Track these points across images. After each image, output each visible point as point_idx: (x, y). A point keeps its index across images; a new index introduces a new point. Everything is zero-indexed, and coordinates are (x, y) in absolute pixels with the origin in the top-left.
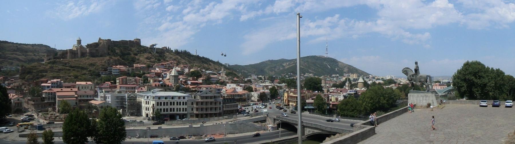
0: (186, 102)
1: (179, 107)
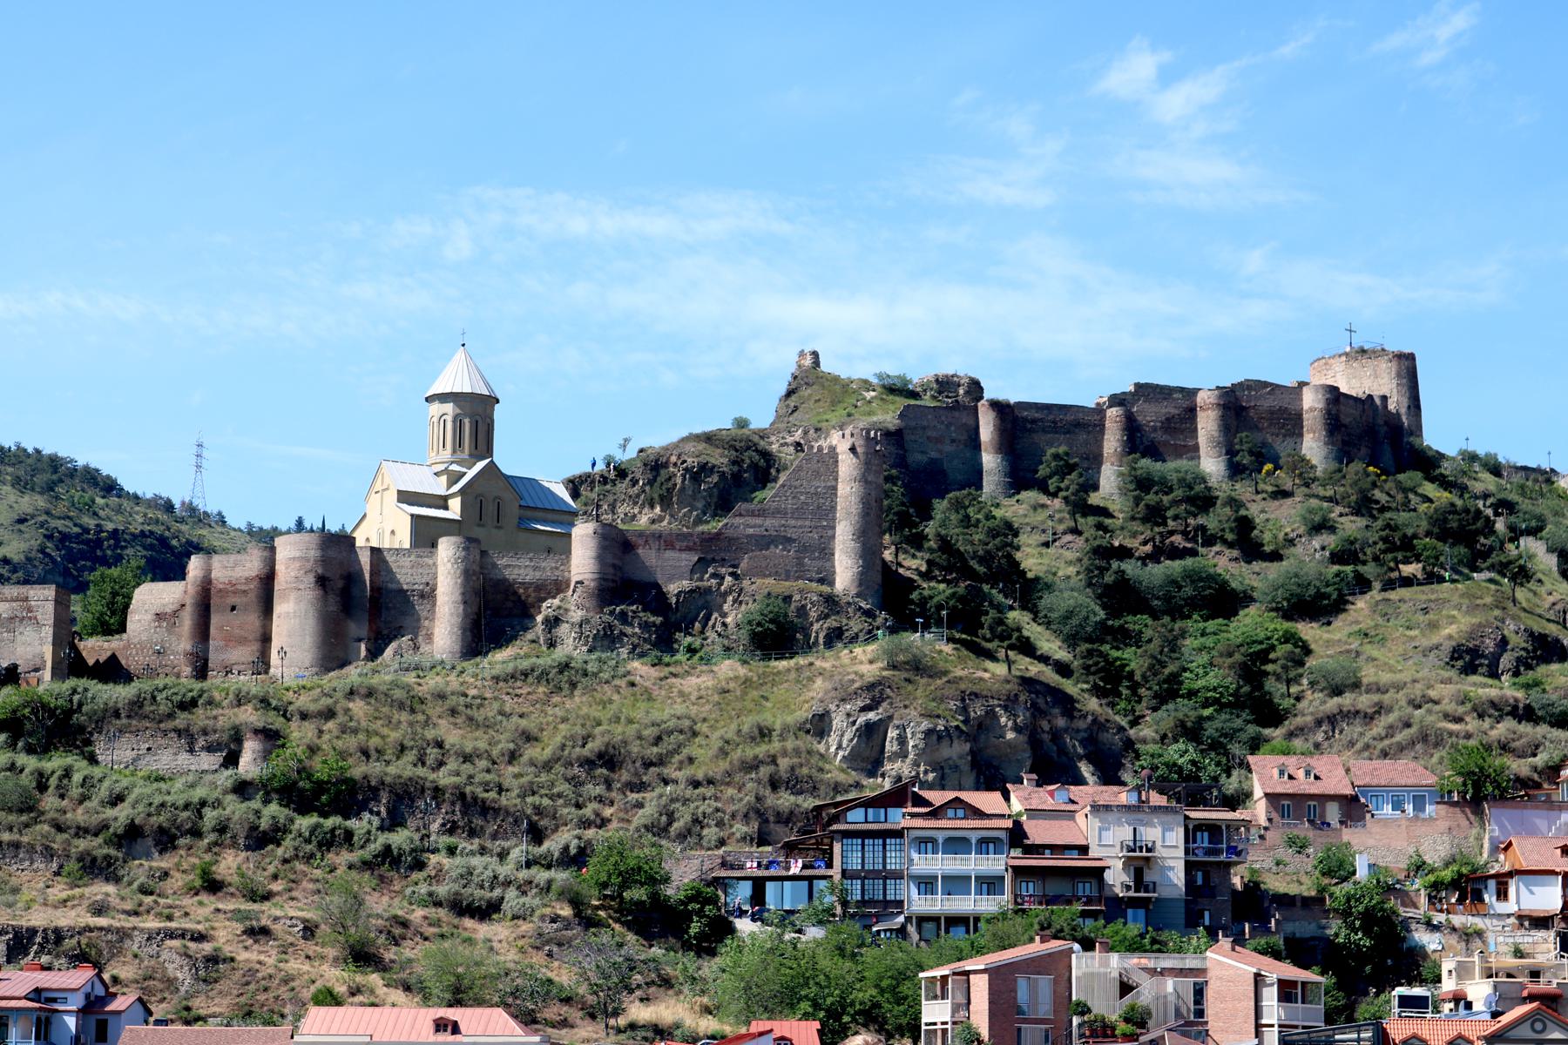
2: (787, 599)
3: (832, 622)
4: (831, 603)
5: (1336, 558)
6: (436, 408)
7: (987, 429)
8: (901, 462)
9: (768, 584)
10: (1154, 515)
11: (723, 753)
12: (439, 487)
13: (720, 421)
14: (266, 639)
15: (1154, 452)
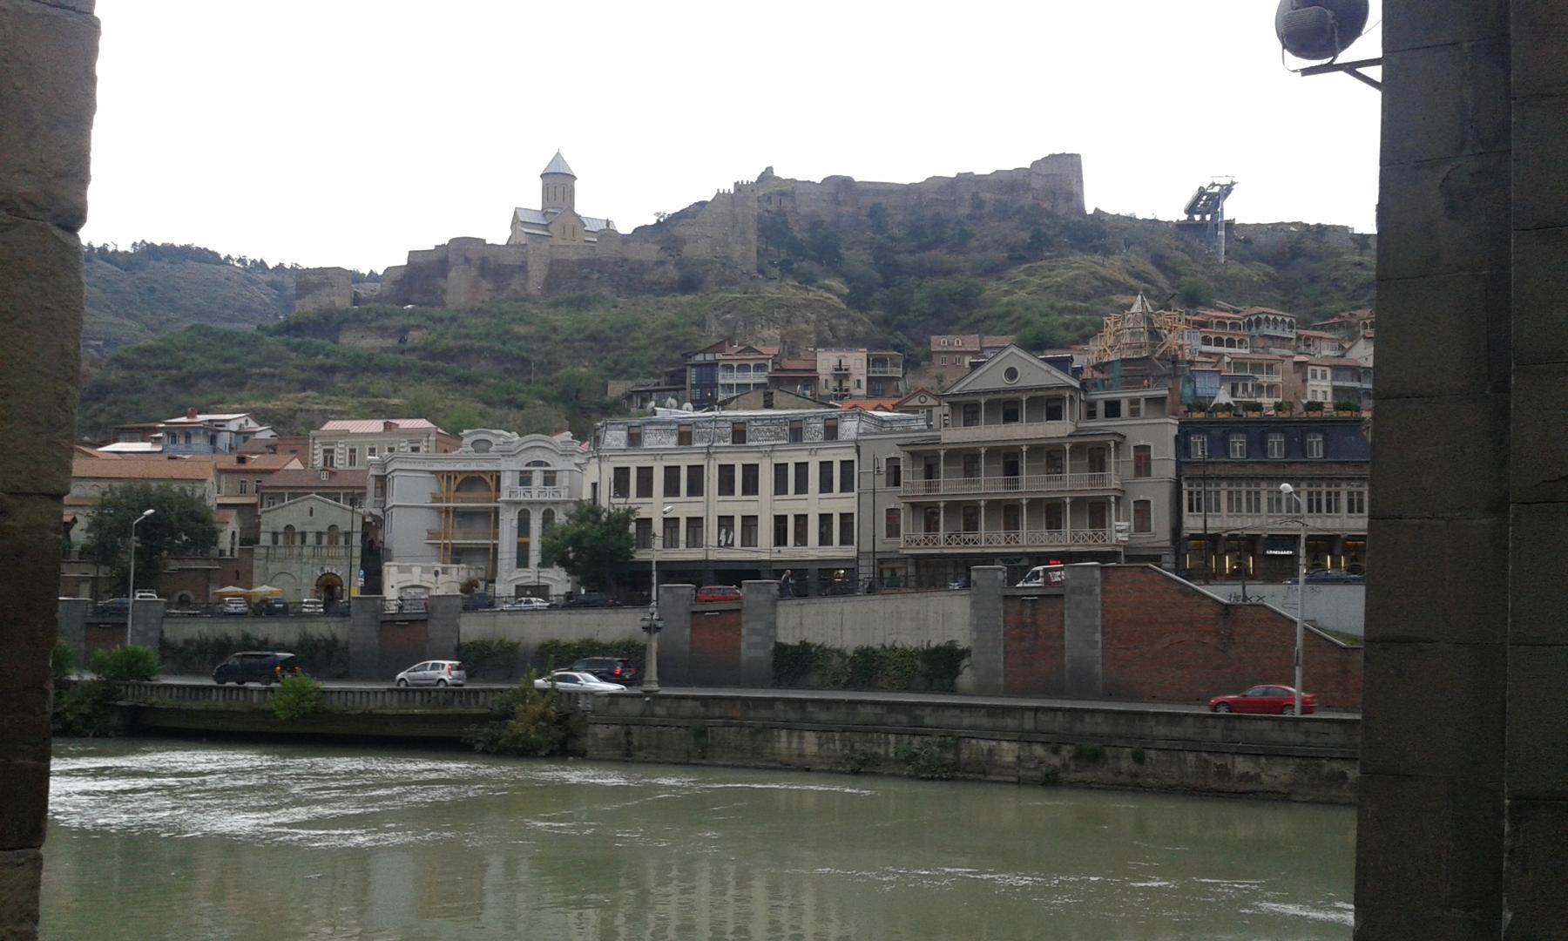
0: (847, 466)
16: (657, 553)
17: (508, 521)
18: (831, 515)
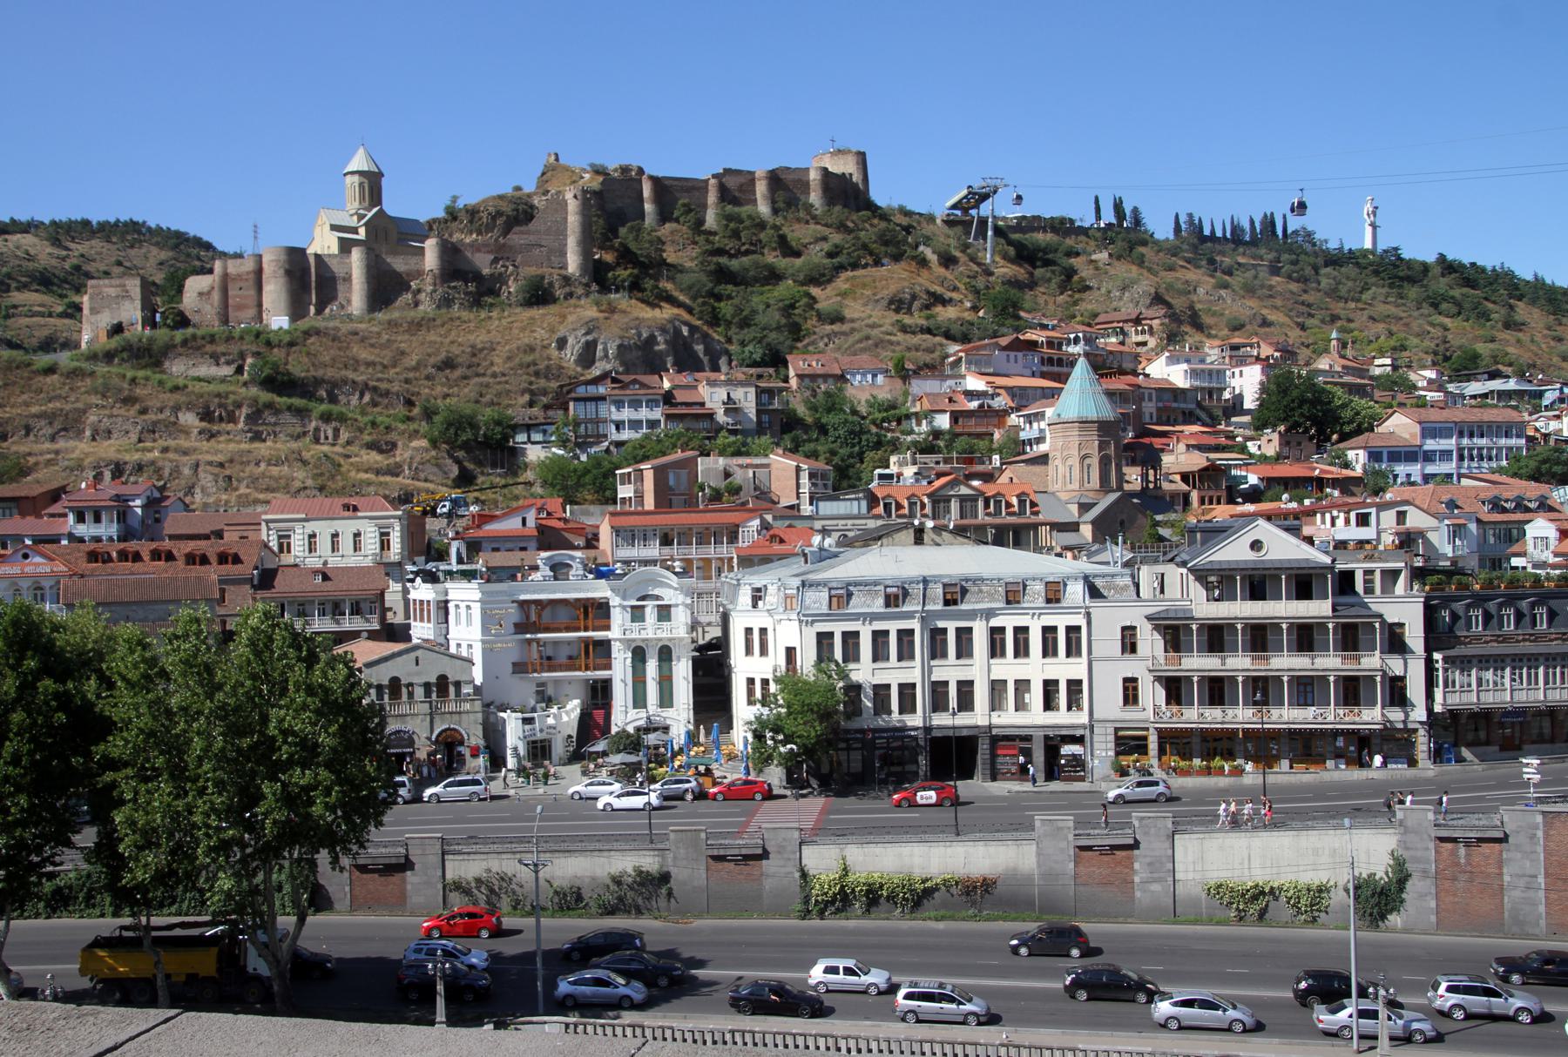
0: (1073, 631)
1: (1008, 669)
2: (543, 278)
3: (567, 289)
4: (567, 280)
5: (830, 255)
6: (349, 179)
7: (647, 191)
8: (601, 207)
9: (532, 271)
10: (736, 234)
11: (509, 358)
12: (353, 222)
13: (507, 190)
14: (260, 305)
15: (736, 202)
16: (868, 721)
17: (621, 661)
18: (1057, 682)
